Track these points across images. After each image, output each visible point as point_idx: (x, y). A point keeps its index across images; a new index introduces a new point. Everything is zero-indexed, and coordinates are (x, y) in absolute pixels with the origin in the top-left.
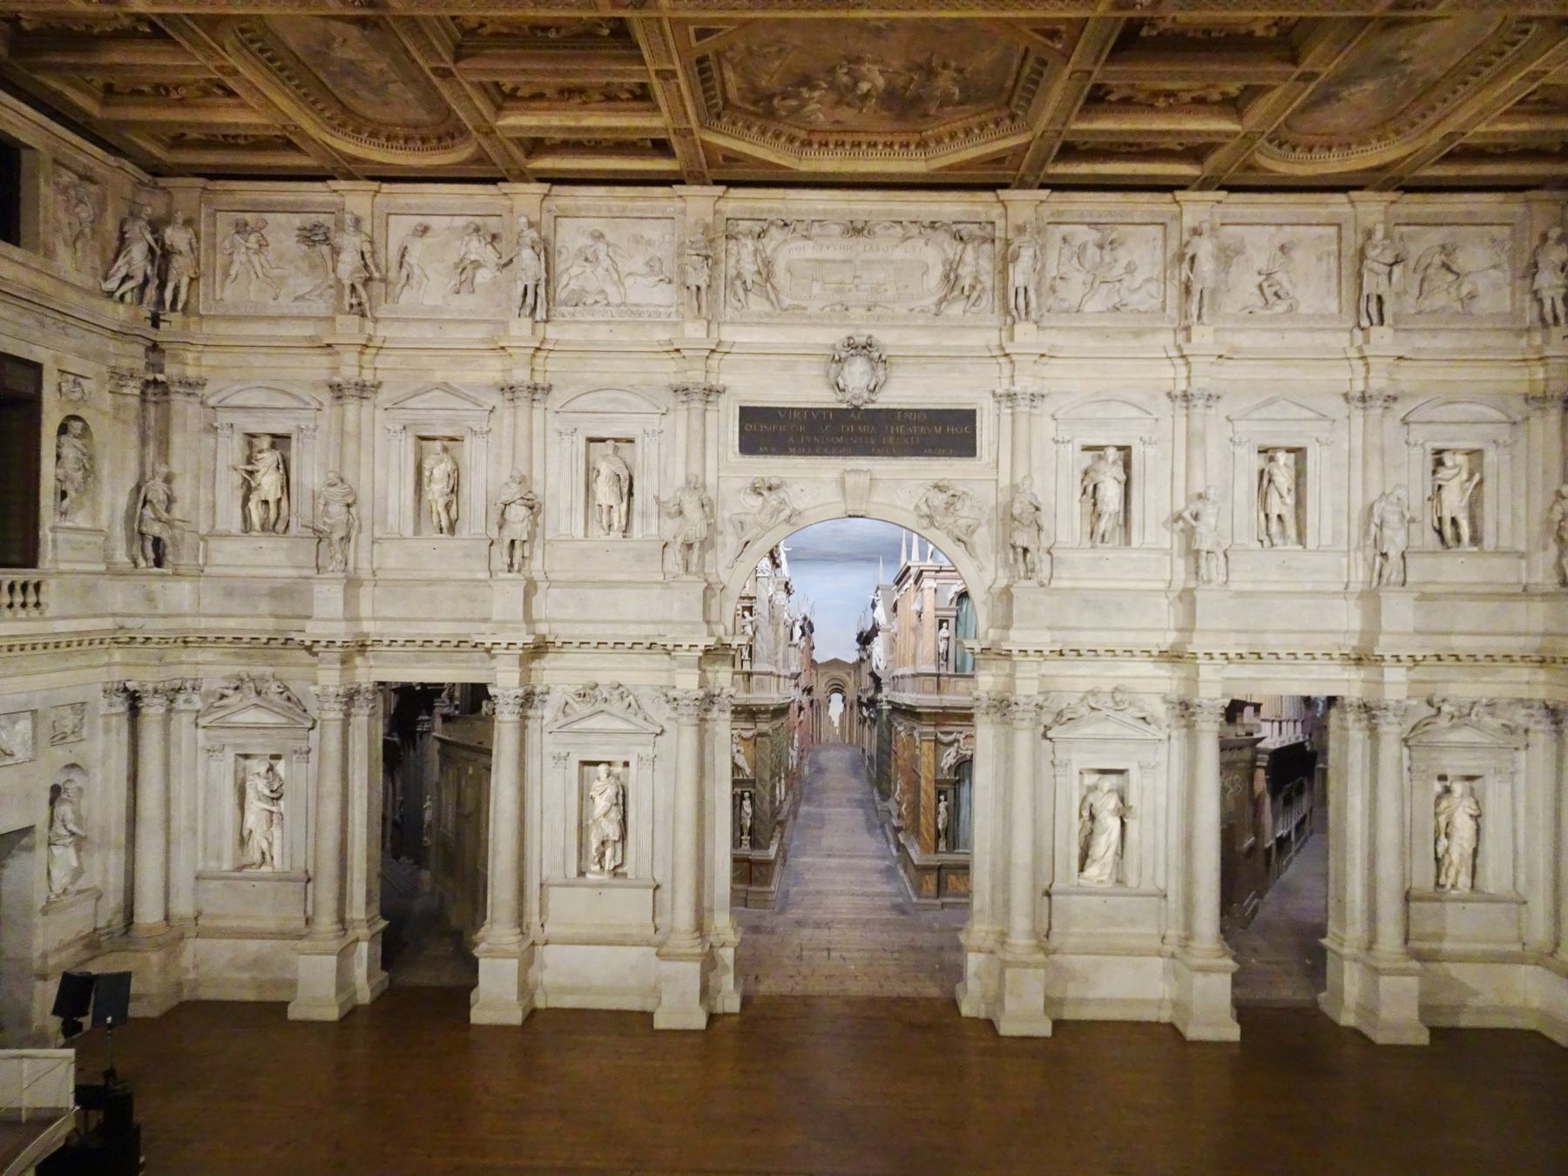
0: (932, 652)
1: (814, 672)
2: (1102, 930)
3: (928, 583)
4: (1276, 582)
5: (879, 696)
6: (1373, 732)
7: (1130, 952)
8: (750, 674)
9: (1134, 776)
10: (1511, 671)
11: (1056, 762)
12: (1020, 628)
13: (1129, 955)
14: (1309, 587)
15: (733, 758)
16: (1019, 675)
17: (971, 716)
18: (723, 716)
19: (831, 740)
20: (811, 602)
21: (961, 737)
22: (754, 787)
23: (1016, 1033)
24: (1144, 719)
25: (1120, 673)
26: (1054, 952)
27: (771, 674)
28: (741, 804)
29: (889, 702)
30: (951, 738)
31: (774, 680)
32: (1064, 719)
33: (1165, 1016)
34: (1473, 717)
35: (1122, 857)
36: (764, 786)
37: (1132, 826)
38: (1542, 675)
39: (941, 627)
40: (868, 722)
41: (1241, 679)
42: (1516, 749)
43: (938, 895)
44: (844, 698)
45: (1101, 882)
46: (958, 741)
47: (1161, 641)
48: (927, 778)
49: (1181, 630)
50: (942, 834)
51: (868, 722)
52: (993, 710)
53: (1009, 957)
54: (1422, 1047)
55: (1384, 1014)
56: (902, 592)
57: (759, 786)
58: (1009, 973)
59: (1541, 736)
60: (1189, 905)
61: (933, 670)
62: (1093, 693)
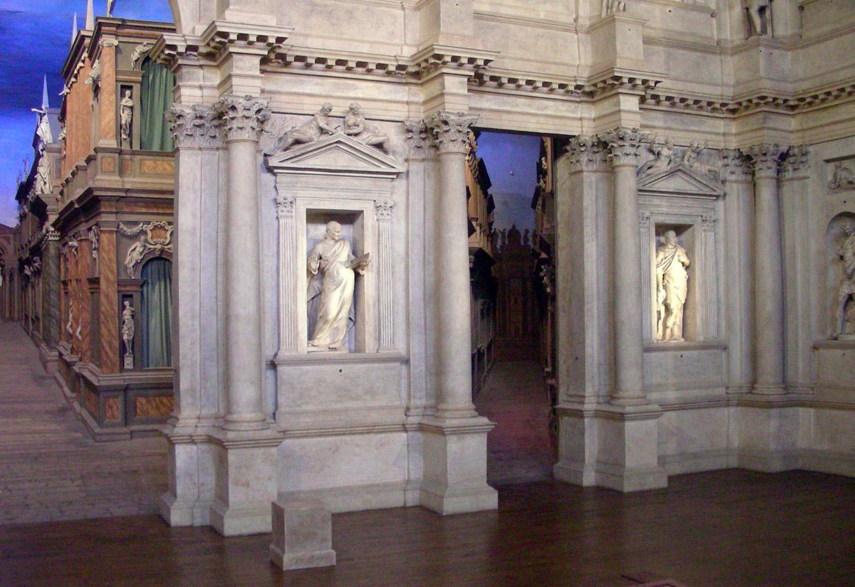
0: (113, 124)
2: (339, 406)
3: (107, 41)
4: (511, 7)
6: (610, 171)
7: (371, 429)
9: (369, 219)
10: (710, 122)
11: (280, 199)
12: (240, 11)
13: (368, 433)
14: (542, 16)
16: (235, 71)
23: (245, 531)
24: (379, 146)
25: (352, 94)
26: (285, 433)
30: (136, 229)
32: (290, 141)
33: (412, 498)
34: (686, 162)
35: (355, 324)
37: (369, 276)
38: (734, 128)
39: (123, 95)
41: (481, 109)
42: (718, 197)
43: (126, 422)
45: (335, 349)
47: (400, 54)
48: (107, 280)
49: (418, 46)
50: (129, 350)
52: (199, 131)
53: (231, 435)
54: (662, 489)
55: (630, 462)
56: (73, 79)
58: (233, 456)
59: (735, 186)
60: (438, 367)
61: (113, 144)
62: (326, 112)
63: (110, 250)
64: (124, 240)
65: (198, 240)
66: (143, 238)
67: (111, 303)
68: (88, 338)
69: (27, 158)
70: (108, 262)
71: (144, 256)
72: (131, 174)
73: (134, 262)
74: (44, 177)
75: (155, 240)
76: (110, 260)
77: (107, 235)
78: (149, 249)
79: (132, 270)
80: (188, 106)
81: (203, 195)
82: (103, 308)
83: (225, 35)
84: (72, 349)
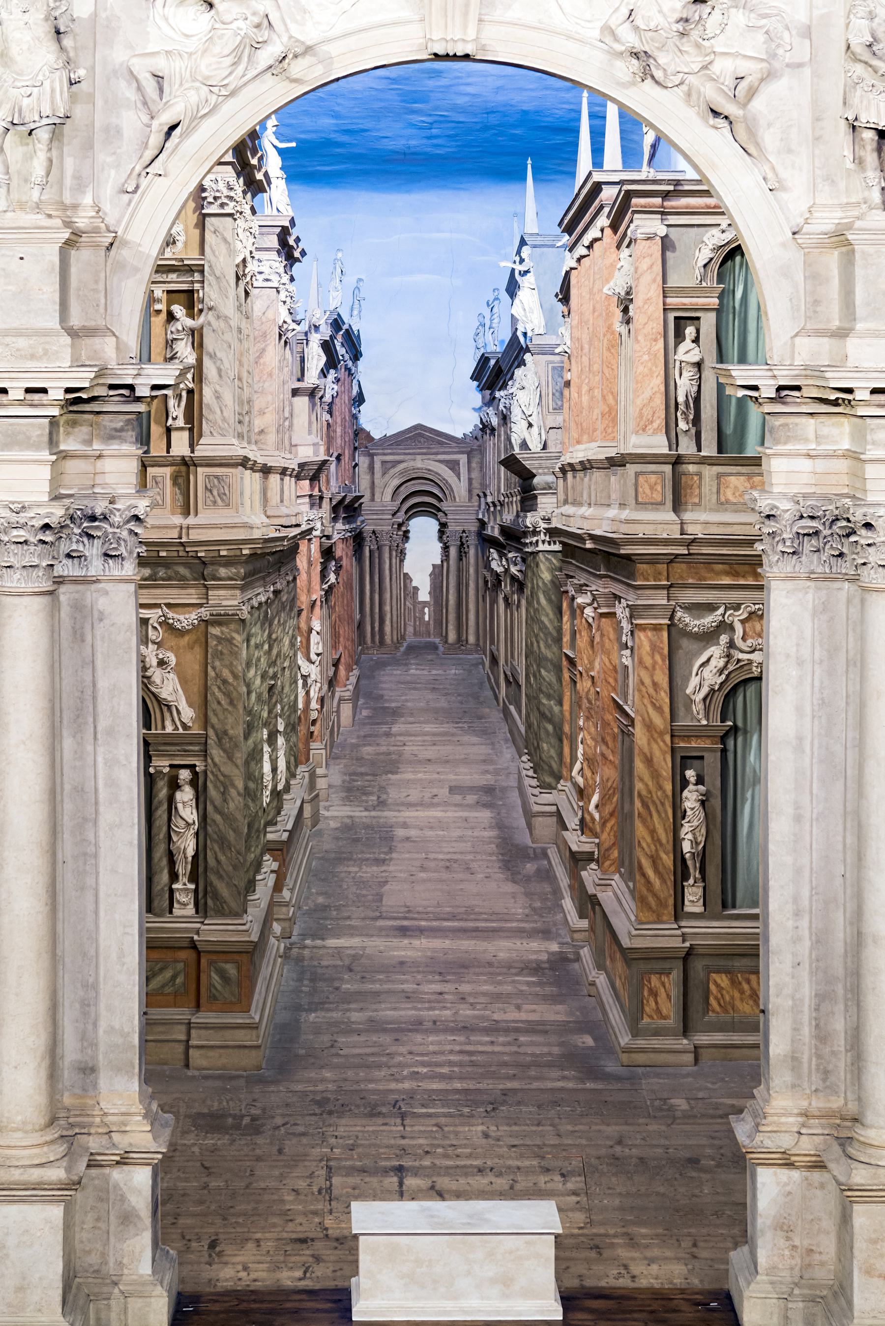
1: (363, 461)
5: (530, 520)
8: (187, 465)
12: (876, 334)
15: (145, 681)
17: (754, 563)
18: (115, 569)
19: (410, 639)
20: (350, 280)
21: (736, 618)
22: (205, 754)
27: (244, 462)
28: (171, 800)
29: (553, 533)
30: (709, 620)
31: (250, 481)
36: (230, 758)
40: (506, 587)
44: (443, 525)
46: (731, 628)
48: (649, 726)
51: (506, 587)
52: (809, 545)
57: (216, 753)
63: (655, 663)
64: (685, 643)
65: (807, 760)
66: (724, 639)
67: (656, 775)
68: (613, 822)
69: (496, 299)
70: (651, 691)
71: (728, 676)
72: (698, 505)
73: (705, 690)
74: (528, 413)
75: (750, 642)
76: (655, 685)
77: (649, 634)
78: (739, 661)
79: (701, 706)
80: (785, 495)
81: (817, 674)
82: (639, 786)
83: (850, 391)
84: (582, 821)
